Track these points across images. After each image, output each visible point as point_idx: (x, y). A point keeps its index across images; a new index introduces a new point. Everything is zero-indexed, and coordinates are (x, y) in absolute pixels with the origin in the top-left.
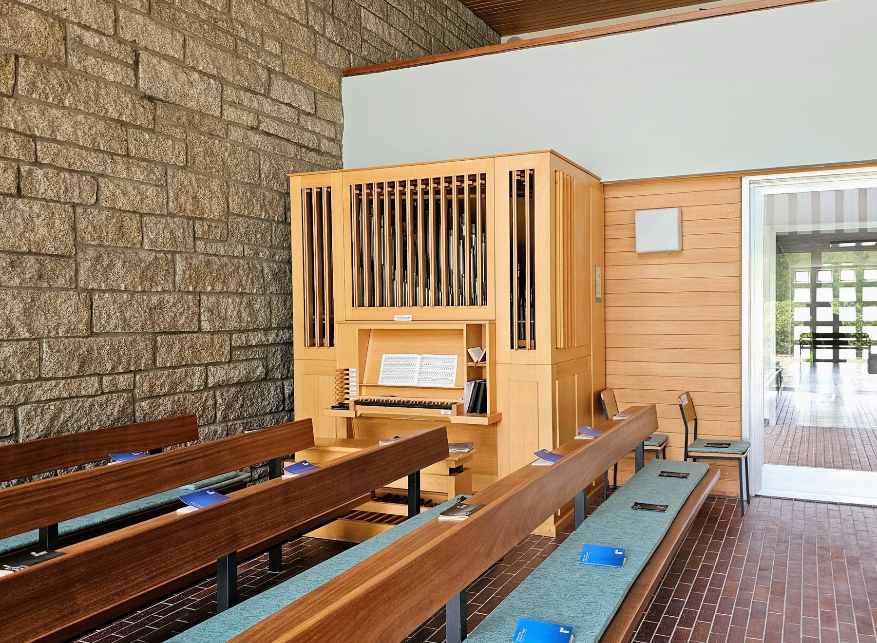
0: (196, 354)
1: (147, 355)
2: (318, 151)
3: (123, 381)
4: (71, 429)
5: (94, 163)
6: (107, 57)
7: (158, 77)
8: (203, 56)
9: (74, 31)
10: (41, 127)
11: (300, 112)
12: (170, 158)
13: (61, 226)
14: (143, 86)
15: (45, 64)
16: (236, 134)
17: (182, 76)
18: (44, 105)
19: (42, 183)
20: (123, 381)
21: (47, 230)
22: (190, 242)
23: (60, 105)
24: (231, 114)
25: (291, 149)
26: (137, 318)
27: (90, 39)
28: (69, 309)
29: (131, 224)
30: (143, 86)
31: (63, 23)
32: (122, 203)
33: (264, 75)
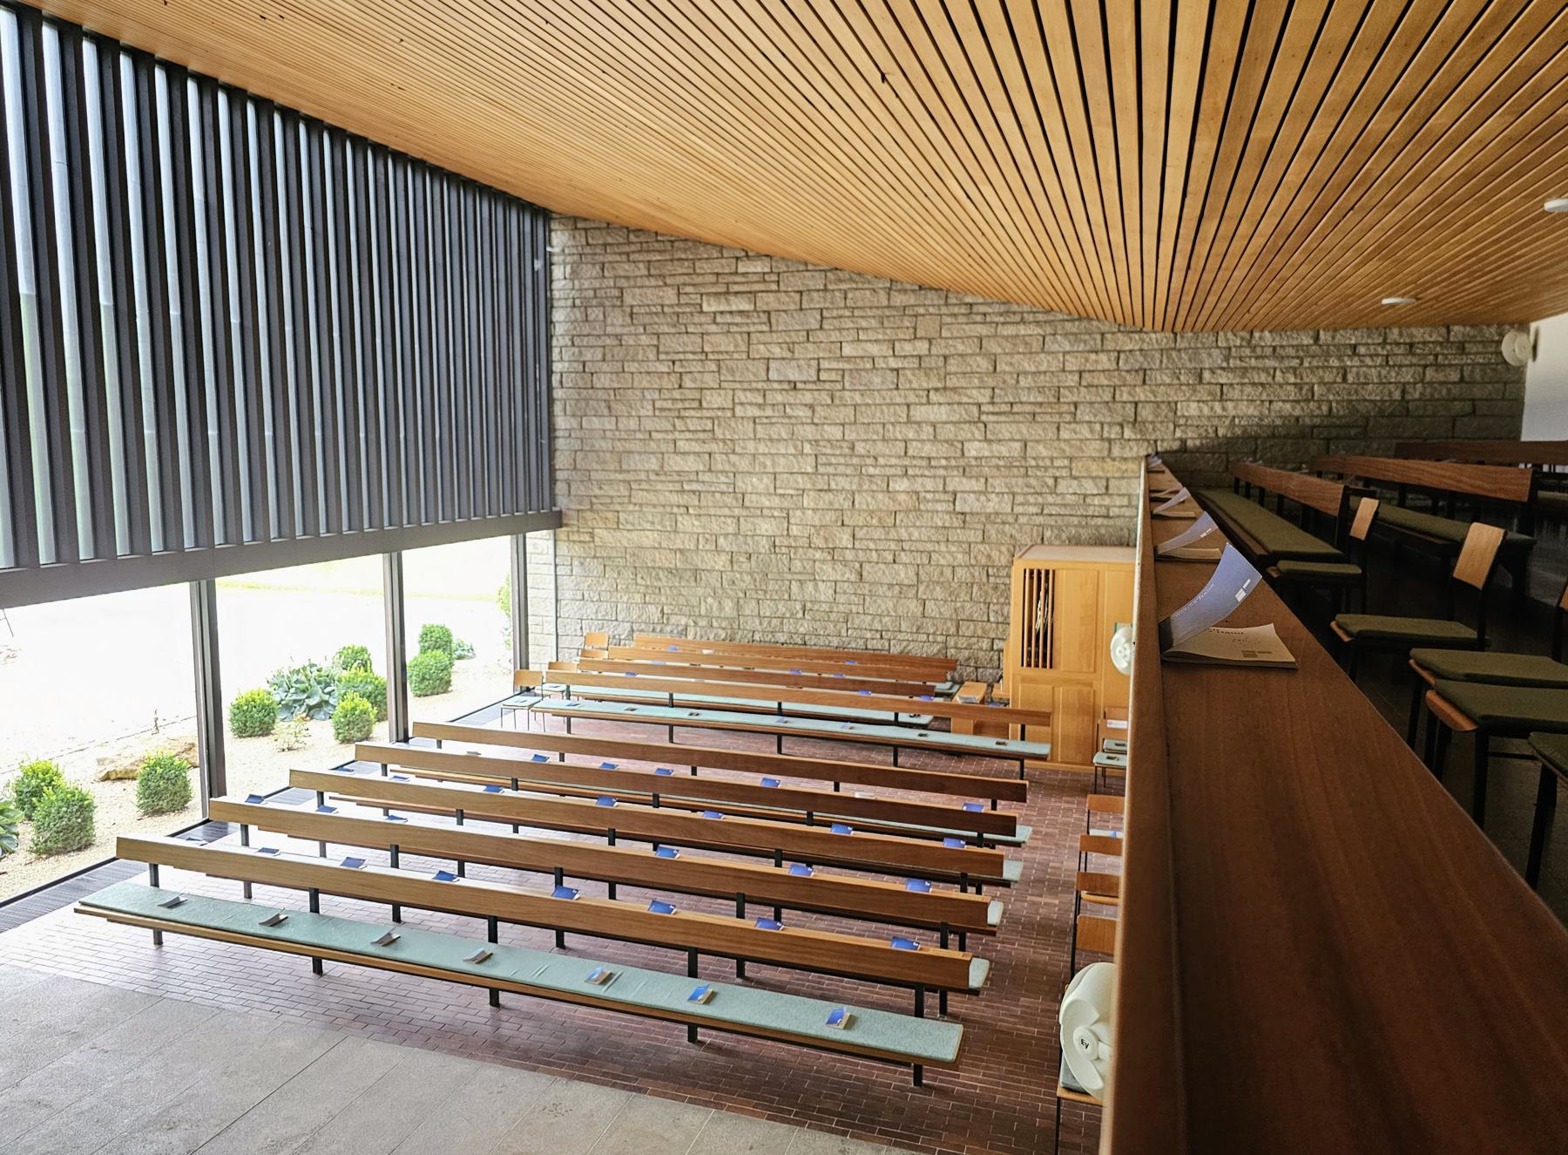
0: (984, 631)
1: (953, 630)
2: (1107, 517)
3: (940, 639)
4: (914, 652)
5: (930, 547)
6: (938, 501)
7: (967, 503)
8: (998, 484)
9: (922, 495)
10: (905, 536)
11: (1085, 496)
12: (972, 539)
13: (911, 573)
14: (958, 509)
15: (907, 511)
16: (1022, 520)
17: (983, 498)
18: (907, 527)
19: (904, 557)
20: (940, 639)
21: (905, 575)
22: (984, 579)
23: (914, 526)
24: (1018, 509)
25: (1076, 521)
26: (947, 611)
27: (929, 496)
28: (914, 607)
29: (948, 572)
30: (958, 509)
31: (917, 493)
32: (942, 562)
33: (1051, 482)
